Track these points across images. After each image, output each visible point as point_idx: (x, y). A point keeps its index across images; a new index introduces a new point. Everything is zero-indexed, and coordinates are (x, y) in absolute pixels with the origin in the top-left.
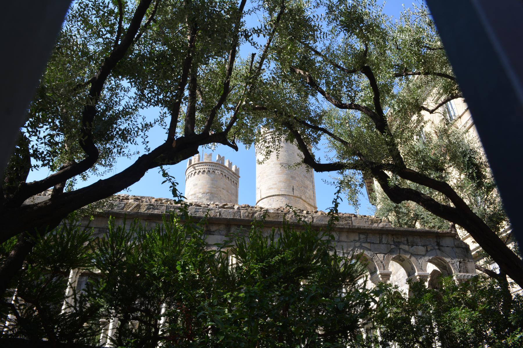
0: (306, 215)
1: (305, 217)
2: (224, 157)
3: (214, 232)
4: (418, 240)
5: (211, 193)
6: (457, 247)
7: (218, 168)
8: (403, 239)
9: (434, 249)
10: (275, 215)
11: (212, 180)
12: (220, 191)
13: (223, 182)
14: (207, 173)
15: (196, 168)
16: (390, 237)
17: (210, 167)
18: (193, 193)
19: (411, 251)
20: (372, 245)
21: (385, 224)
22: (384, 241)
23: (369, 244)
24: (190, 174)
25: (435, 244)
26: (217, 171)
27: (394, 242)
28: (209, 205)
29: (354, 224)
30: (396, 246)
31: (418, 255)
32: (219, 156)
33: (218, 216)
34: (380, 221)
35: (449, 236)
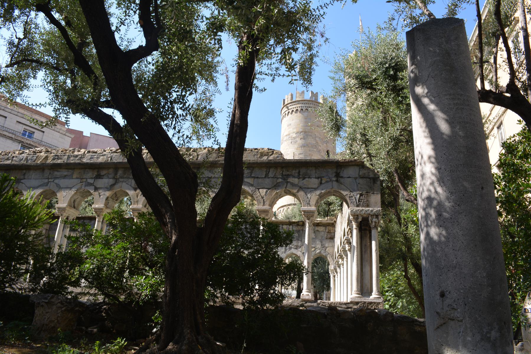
2: (317, 93)
3: (103, 176)
4: (312, 172)
5: (305, 132)
6: (362, 177)
7: (311, 106)
8: (294, 171)
9: (331, 180)
11: (306, 119)
14: (300, 112)
15: (290, 108)
16: (279, 170)
17: (303, 105)
18: (286, 133)
19: (300, 184)
20: (256, 179)
21: (276, 156)
22: (271, 175)
23: (253, 179)
25: (334, 175)
27: (282, 175)
30: (284, 179)
32: (312, 92)
34: (271, 153)
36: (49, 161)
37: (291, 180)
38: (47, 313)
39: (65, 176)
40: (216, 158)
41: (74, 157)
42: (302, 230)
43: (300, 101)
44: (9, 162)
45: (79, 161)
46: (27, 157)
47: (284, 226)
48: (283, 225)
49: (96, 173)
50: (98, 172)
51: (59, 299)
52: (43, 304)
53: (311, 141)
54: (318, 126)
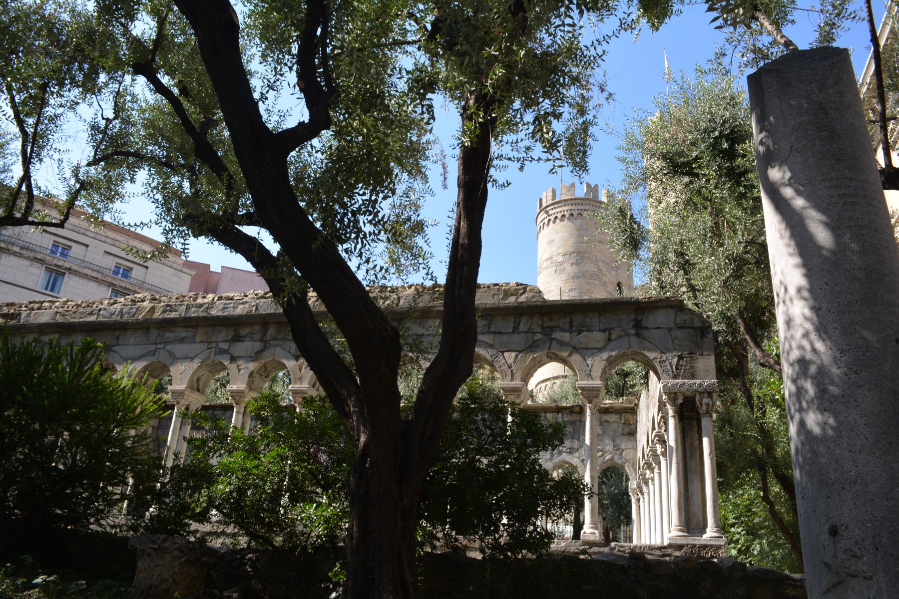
2: (597, 186)
3: (244, 336)
4: (594, 320)
5: (579, 253)
6: (681, 328)
7: (587, 207)
8: (562, 321)
9: (627, 335)
11: (579, 230)
14: (569, 219)
15: (551, 212)
16: (536, 319)
17: (573, 207)
18: (547, 256)
20: (497, 336)
21: (531, 295)
22: (523, 327)
23: (492, 336)
25: (632, 324)
27: (542, 327)
30: (546, 335)
31: (588, 349)
32: (588, 185)
35: (664, 307)
36: (157, 315)
37: (557, 335)
38: (156, 566)
39: (183, 338)
41: (196, 307)
42: (580, 421)
43: (565, 200)
44: (92, 318)
45: (204, 314)
46: (122, 309)
47: (548, 415)
48: (546, 412)
49: (232, 333)
51: (176, 543)
52: (150, 551)
53: (589, 267)
54: (600, 242)
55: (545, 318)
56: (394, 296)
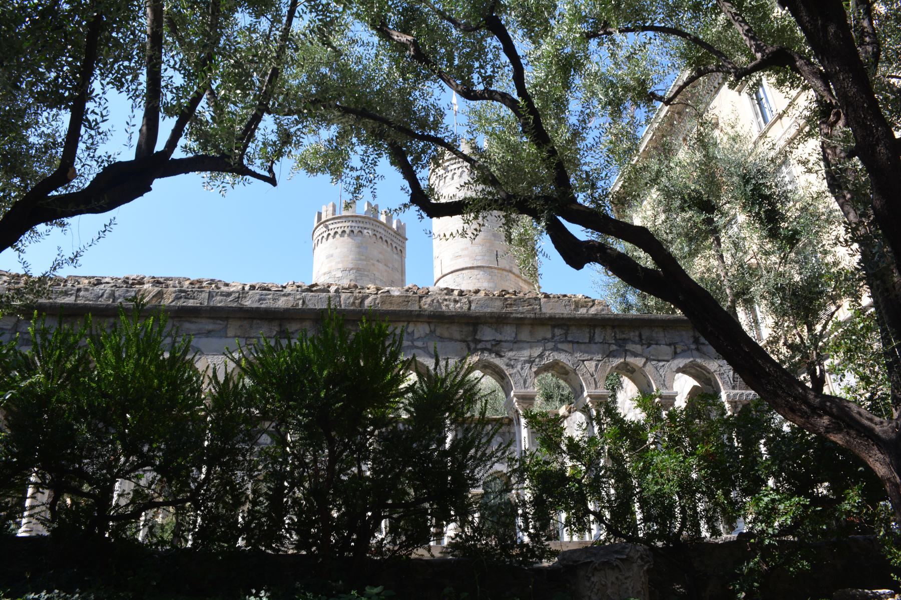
0: (457, 298)
1: (456, 301)
3: (293, 333)
4: (659, 334)
5: (358, 270)
7: (368, 226)
8: (632, 334)
9: (689, 349)
10: (401, 299)
12: (373, 265)
13: (378, 250)
14: (349, 235)
15: (330, 227)
16: (609, 331)
18: (326, 270)
21: (600, 308)
22: (598, 338)
23: (571, 345)
24: (320, 238)
25: (691, 340)
26: (366, 231)
27: (616, 339)
28: (285, 287)
29: (544, 310)
30: (620, 346)
33: (300, 306)
34: (591, 304)
36: (168, 301)
37: (630, 347)
38: (626, 579)
39: (209, 332)
40: (503, 308)
41: (222, 295)
42: (509, 432)
44: (69, 300)
45: (235, 305)
46: (113, 292)
49: (277, 329)
50: (280, 325)
51: (638, 551)
52: (618, 563)
54: (378, 261)
55: (617, 330)
56: (464, 300)
